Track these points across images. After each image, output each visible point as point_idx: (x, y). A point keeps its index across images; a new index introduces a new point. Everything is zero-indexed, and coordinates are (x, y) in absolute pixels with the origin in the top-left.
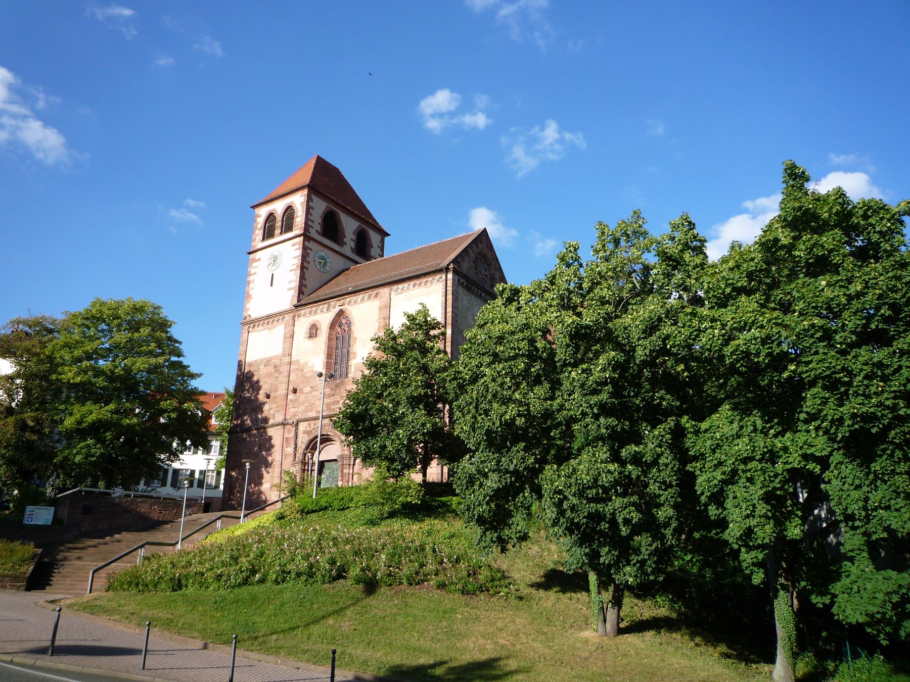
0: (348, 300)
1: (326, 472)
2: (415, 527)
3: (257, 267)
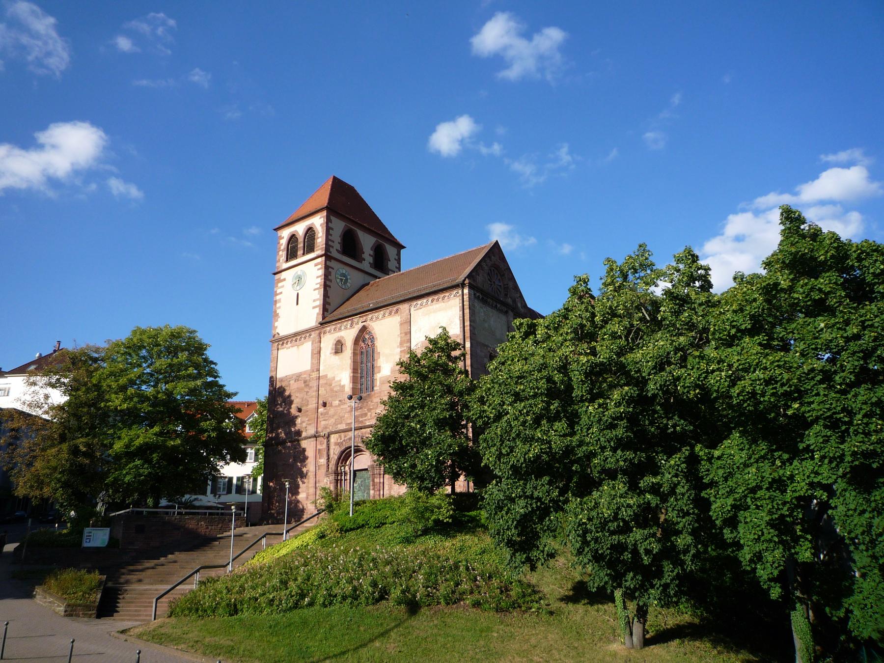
0: (370, 316)
1: (359, 481)
2: (448, 544)
3: (283, 286)
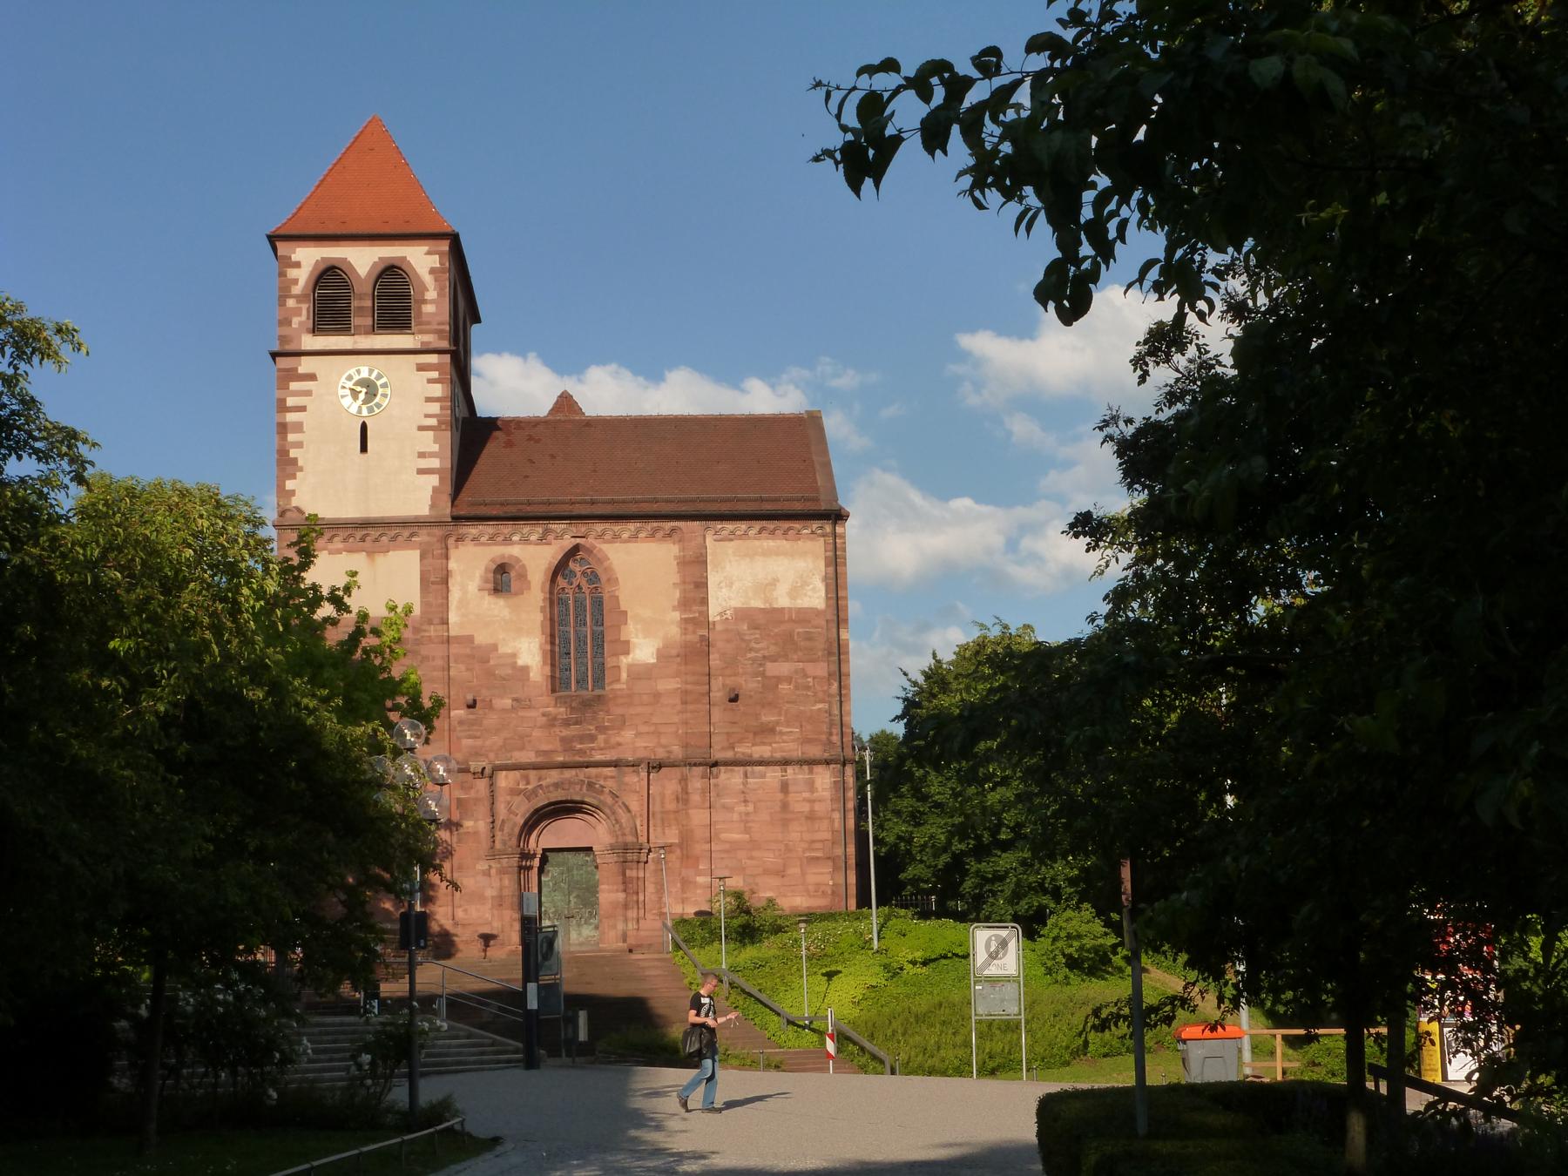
1: (553, 871)
3: (308, 393)
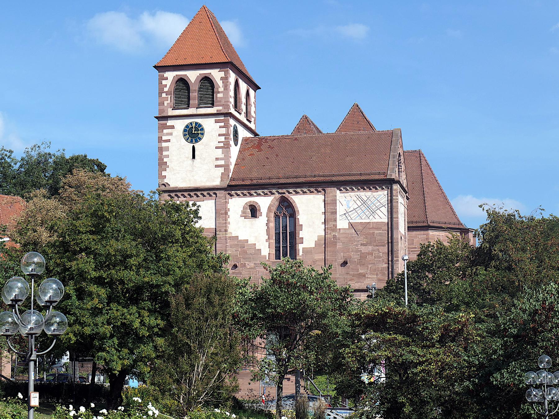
3: (171, 134)
